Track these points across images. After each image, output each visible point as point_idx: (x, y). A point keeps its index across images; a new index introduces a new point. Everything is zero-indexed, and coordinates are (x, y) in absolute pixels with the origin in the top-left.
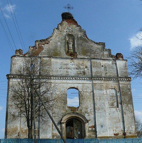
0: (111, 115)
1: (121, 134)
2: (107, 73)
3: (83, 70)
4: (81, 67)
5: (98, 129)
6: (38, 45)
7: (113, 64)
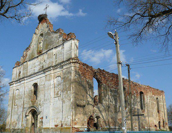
0: (54, 105)
1: (60, 125)
2: (57, 61)
3: (42, 65)
4: (42, 62)
5: (44, 120)
6: (26, 53)
7: (62, 49)
